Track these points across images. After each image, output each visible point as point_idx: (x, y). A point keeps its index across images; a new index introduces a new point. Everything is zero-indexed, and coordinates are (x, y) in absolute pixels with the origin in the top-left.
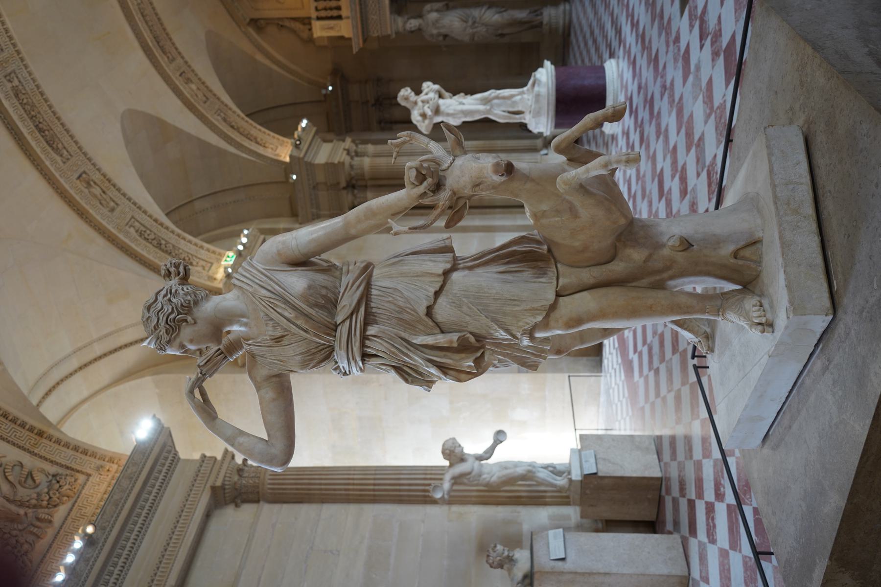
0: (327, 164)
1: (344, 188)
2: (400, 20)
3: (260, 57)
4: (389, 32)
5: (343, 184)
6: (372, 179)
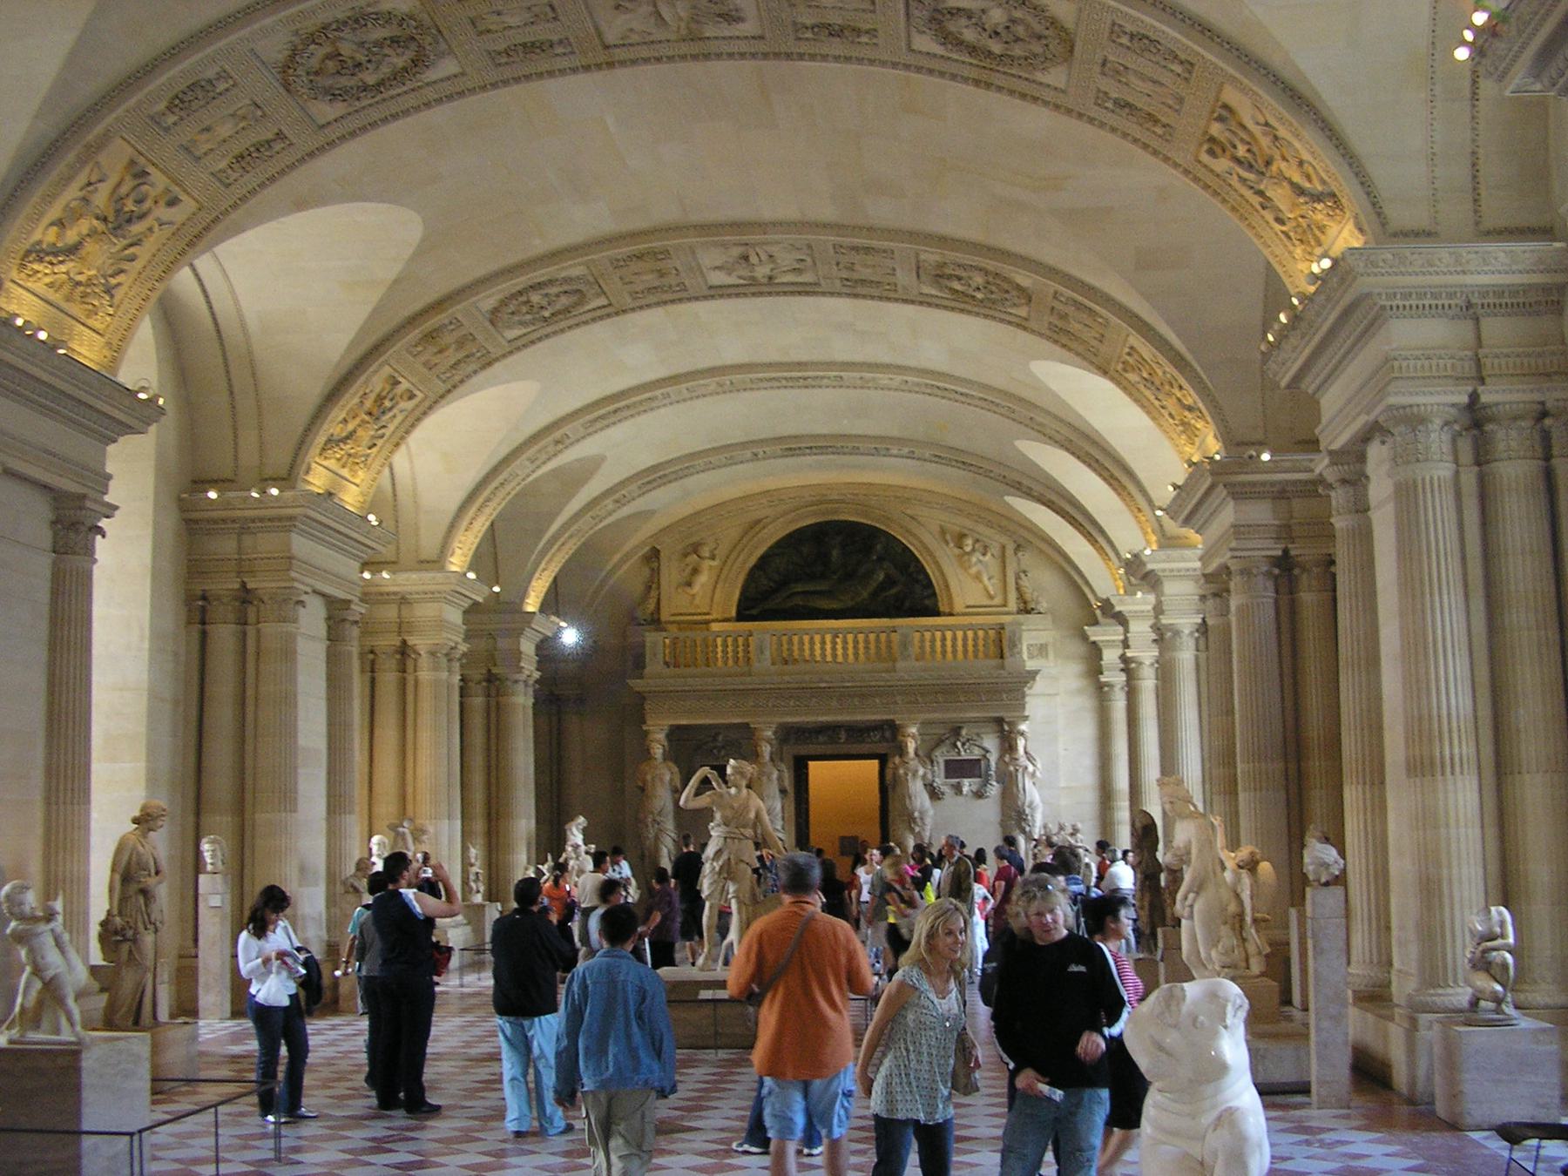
0: (521, 653)
1: (489, 671)
2: (661, 736)
3: (617, 557)
4: (649, 722)
5: (495, 671)
6: (498, 703)
